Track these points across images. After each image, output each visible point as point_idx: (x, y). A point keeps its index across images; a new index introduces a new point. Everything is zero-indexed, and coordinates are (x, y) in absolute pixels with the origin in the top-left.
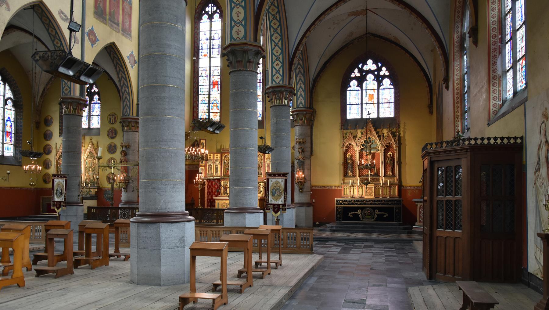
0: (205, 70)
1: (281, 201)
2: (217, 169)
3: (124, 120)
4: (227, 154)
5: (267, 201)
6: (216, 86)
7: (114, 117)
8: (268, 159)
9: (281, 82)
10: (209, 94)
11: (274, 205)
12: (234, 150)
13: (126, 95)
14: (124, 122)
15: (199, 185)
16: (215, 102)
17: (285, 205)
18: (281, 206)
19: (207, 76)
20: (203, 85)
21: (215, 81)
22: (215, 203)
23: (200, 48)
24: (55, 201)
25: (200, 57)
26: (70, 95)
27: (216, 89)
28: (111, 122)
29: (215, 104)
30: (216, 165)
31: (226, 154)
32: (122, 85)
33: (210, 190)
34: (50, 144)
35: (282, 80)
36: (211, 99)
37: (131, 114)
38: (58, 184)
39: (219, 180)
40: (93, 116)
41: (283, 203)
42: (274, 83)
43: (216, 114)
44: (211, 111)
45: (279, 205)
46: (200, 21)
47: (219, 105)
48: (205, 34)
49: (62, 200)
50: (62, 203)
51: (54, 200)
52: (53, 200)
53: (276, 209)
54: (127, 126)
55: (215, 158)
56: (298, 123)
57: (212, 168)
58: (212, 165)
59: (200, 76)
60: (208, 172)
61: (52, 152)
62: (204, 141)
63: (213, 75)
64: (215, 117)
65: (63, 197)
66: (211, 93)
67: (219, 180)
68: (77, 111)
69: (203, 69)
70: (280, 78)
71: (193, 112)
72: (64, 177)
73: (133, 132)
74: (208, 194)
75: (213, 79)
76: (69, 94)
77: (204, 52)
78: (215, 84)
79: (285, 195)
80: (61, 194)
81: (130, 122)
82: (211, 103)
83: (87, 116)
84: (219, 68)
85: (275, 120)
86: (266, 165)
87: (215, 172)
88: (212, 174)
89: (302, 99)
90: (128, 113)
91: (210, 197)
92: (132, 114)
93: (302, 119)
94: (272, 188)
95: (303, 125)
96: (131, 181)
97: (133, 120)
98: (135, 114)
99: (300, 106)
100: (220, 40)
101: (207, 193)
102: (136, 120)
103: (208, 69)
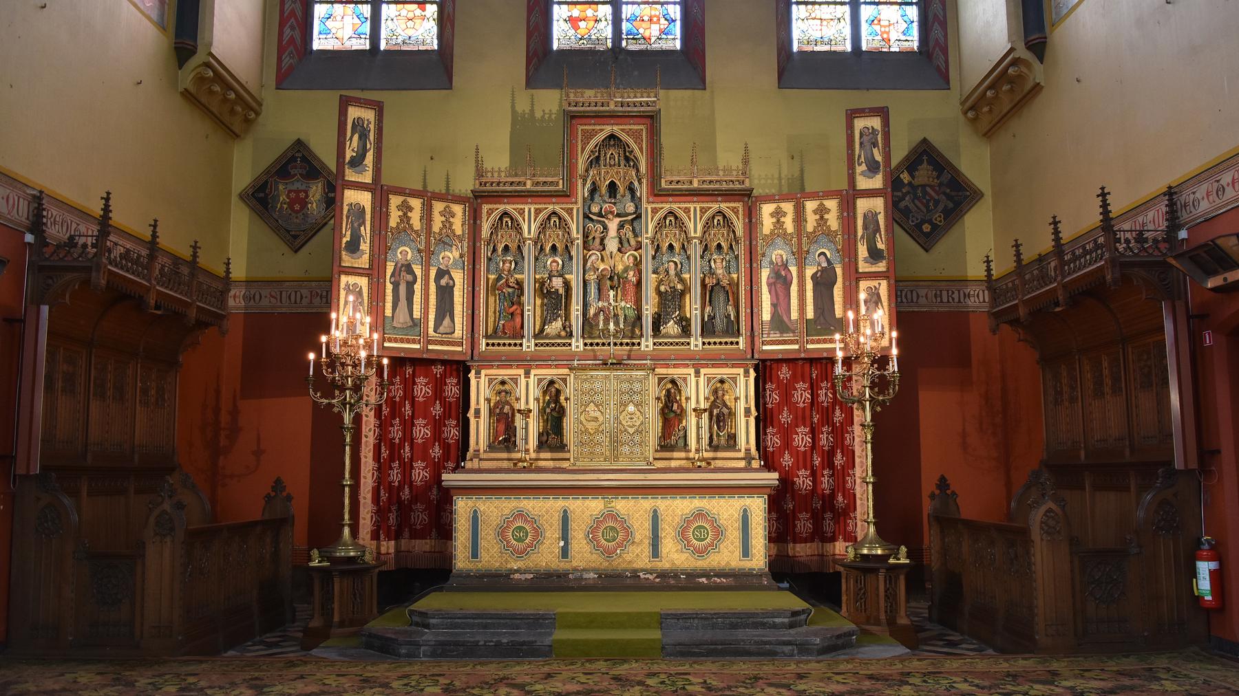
2: (445, 294)
4: (509, 208)
15: (343, 389)
30: (441, 274)
31: (502, 207)
33: (396, 433)
39: (460, 369)
55: (437, 225)
57: (417, 287)
58: (418, 270)
60: (388, 312)
64: (410, 24)
67: (460, 369)
74: (385, 453)
86: (765, 274)
87: (432, 316)
88: (415, 324)
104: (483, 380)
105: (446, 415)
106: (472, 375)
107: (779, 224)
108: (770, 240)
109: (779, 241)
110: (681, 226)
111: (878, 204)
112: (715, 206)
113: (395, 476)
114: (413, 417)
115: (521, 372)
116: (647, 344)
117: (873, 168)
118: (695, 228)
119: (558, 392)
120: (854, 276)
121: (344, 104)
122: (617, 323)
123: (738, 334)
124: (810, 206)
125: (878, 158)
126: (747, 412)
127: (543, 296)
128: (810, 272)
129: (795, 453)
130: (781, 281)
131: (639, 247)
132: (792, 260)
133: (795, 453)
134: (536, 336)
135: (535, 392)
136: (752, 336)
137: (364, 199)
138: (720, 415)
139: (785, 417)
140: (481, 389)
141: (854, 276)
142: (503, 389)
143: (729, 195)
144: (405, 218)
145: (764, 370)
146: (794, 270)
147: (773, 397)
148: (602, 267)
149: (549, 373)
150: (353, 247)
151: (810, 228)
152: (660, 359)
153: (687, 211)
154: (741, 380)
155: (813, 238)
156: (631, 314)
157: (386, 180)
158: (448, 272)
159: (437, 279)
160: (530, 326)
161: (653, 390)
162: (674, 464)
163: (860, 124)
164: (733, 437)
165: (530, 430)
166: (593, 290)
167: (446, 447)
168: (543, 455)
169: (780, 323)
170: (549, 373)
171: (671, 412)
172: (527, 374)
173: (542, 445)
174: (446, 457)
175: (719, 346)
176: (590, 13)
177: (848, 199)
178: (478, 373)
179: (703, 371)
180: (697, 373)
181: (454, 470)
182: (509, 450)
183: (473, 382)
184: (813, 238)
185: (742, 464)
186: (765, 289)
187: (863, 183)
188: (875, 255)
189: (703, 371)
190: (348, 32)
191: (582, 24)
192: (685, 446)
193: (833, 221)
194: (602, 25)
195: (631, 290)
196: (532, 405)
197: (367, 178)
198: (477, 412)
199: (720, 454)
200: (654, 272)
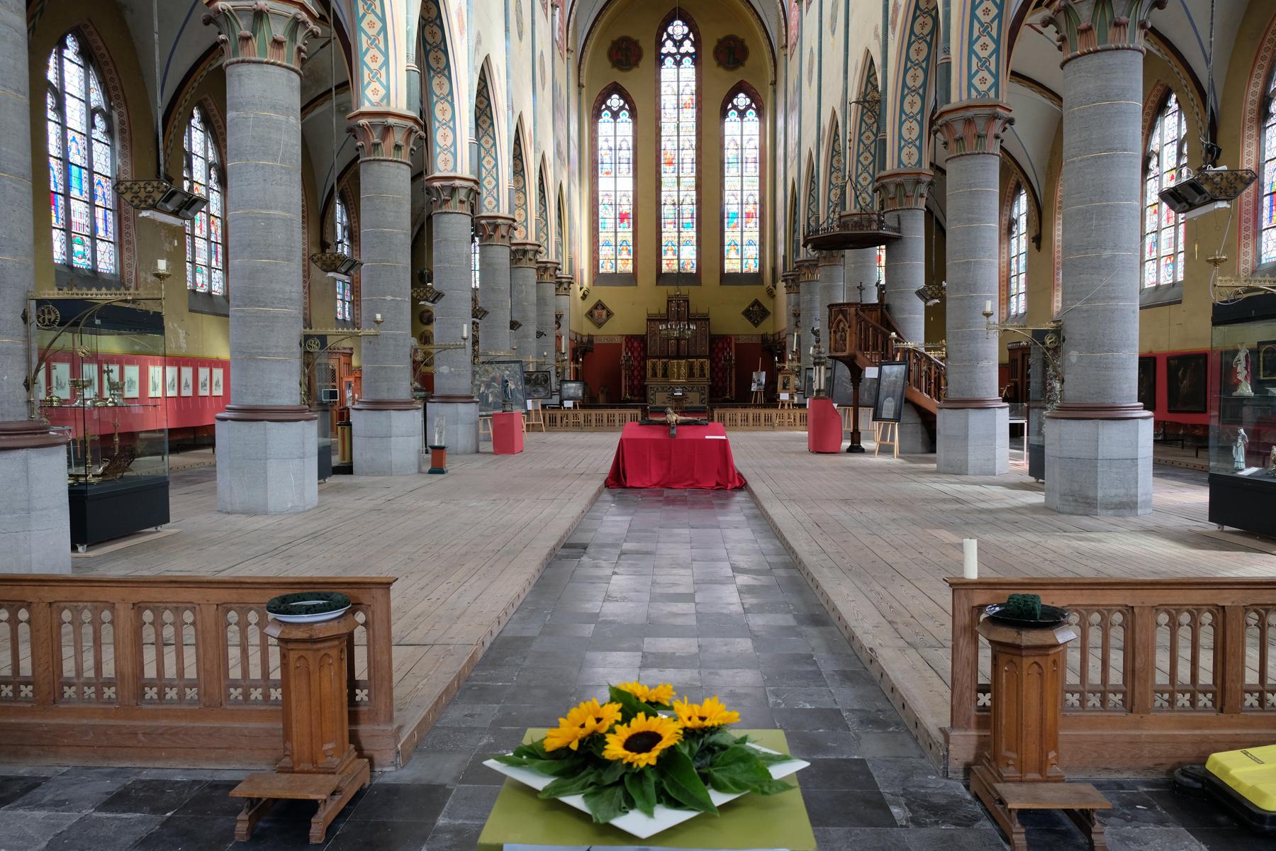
6: (626, 221)
10: (616, 232)
19: (611, 204)
23: (600, 162)
25: (600, 175)
36: (619, 239)
44: (618, 257)
46: (599, 119)
47: (631, 248)
48: (607, 141)
66: (618, 230)
69: (605, 193)
77: (603, 169)
78: (623, 217)
100: (631, 151)
103: (613, 193)
138: (702, 369)
142: (654, 365)
165: (660, 373)
190: (609, 267)
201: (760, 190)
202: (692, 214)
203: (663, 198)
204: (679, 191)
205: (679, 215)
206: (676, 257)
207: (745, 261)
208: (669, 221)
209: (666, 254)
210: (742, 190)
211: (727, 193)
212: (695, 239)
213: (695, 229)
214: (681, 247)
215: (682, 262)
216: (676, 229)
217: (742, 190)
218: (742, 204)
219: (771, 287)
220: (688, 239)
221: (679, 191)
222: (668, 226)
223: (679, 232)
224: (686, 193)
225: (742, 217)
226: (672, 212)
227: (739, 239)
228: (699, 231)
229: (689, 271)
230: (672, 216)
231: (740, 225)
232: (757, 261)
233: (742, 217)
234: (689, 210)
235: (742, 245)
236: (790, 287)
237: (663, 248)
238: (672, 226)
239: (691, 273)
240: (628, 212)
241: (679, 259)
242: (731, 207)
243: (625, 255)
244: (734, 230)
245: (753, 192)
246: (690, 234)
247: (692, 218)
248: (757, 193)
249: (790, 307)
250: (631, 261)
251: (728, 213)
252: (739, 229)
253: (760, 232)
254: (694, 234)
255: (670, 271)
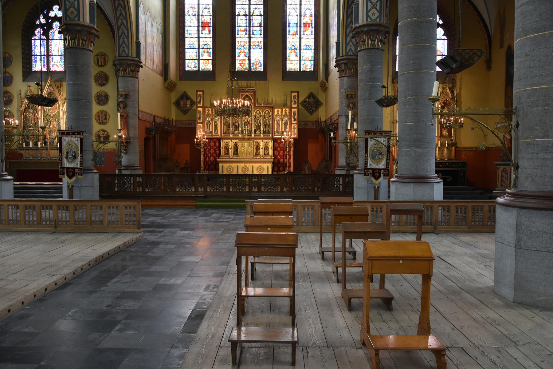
0: (192, 7)
1: (383, 165)
2: (216, 126)
3: (121, 62)
5: (366, 166)
6: (207, 28)
7: (103, 57)
8: (277, 115)
9: (378, 20)
10: (199, 37)
11: (374, 170)
12: (414, 99)
13: (123, 29)
14: (120, 64)
16: (206, 47)
17: (388, 170)
18: (382, 171)
19: (195, 15)
20: (190, 26)
21: (205, 22)
22: (218, 166)
24: (64, 168)
26: (79, 20)
27: (206, 31)
28: (100, 64)
29: (206, 50)
30: (215, 122)
32: (118, 16)
34: (10, 91)
35: (380, 17)
36: (201, 43)
37: (130, 55)
38: (69, 144)
39: (219, 140)
40: (52, 55)
41: (385, 167)
42: (369, 20)
43: (208, 62)
44: (201, 58)
45: (380, 170)
47: (211, 51)
49: (76, 166)
50: (76, 170)
51: (63, 166)
52: (62, 166)
53: (377, 175)
54: (125, 70)
56: (346, 73)
57: (211, 125)
58: (211, 122)
59: (186, 14)
60: (206, 130)
61: (13, 102)
62: (201, 93)
63: (203, 14)
64: (206, 64)
65: (78, 161)
66: (201, 35)
67: (219, 140)
68: (87, 44)
69: (190, 6)
70: (377, 14)
71: (180, 59)
72: (79, 134)
73: (132, 78)
74: (205, 155)
75: (203, 20)
76: (77, 19)
79: (387, 157)
80: (75, 157)
81: (129, 65)
82: (200, 48)
83: (62, 55)
84: (211, 6)
85: (369, 66)
86: (275, 122)
87: (214, 130)
88: (211, 132)
89: (352, 45)
90: (125, 53)
91: (207, 159)
92: (132, 55)
93: (351, 70)
94: (372, 149)
95: (352, 76)
96: (132, 140)
97: (133, 63)
98: (134, 55)
99: (349, 54)
101: (204, 154)
102: (136, 63)
103: (196, 6)
104: (223, 142)
105: (216, 148)
106: (221, 141)
107: (278, 113)
108: (276, 116)
109: (278, 116)
110: (260, 113)
111: (296, 110)
112: (266, 109)
113: (207, 159)
114: (210, 149)
115: (230, 141)
116: (253, 135)
117: (295, 103)
118: (262, 113)
119: (237, 144)
120: (291, 124)
121: (197, 91)
122: (247, 132)
123: (270, 134)
124: (284, 109)
125: (296, 101)
126: (271, 148)
127: (234, 126)
128: (283, 122)
129: (280, 156)
130: (278, 124)
131: (252, 117)
132: (280, 120)
133: (280, 156)
134: (233, 134)
135: (233, 144)
136: (273, 134)
137: (201, 109)
138: (266, 149)
139: (279, 149)
140: (223, 144)
141: (291, 124)
142: (227, 144)
143: (269, 107)
144: (208, 112)
145: (275, 141)
146: (280, 122)
147: (277, 145)
148: (245, 120)
149: (235, 141)
150: (199, 118)
151: (284, 114)
152: (255, 138)
153: (261, 110)
154: (270, 142)
155: (284, 116)
156: (251, 130)
157: (205, 105)
158: (216, 122)
159: (214, 124)
160: (231, 132)
161: (253, 144)
162: (258, 158)
163: (293, 94)
164: (268, 153)
165: (232, 151)
166: (243, 125)
167: (216, 154)
168: (234, 156)
169: (278, 132)
170: (235, 141)
171: (258, 148)
172: (231, 141)
173: (234, 154)
174: (217, 156)
175: (267, 136)
176: (244, 62)
177: (291, 108)
178: (222, 141)
179: (263, 141)
180: (262, 141)
181: (218, 159)
182: (228, 155)
183: (221, 142)
184: (284, 116)
185: (270, 158)
186: (275, 125)
187: (293, 106)
188: (295, 120)
189: (263, 141)
190: (193, 66)
191: (242, 65)
192: (260, 155)
193: (288, 113)
194: (246, 65)
195: (250, 125)
196: (232, 147)
197: (201, 105)
198: (222, 148)
199: (266, 156)
200: (255, 121)
201: (315, 5)
202: (261, 24)
203: (237, 11)
204: (250, 4)
205: (250, 25)
206: (247, 58)
207: (302, 62)
208: (242, 29)
209: (239, 56)
210: (301, 5)
211: (288, 7)
212: (262, 44)
213: (262, 36)
214: (252, 50)
215: (252, 62)
216: (247, 36)
217: (301, 5)
218: (300, 16)
219: (324, 81)
220: (257, 44)
221: (250, 4)
222: (240, 33)
223: (250, 38)
224: (255, 6)
225: (300, 27)
226: (244, 22)
227: (298, 44)
228: (265, 38)
229: (258, 70)
230: (244, 25)
231: (299, 33)
232: (312, 62)
233: (300, 27)
234: (258, 20)
235: (300, 49)
236: (343, 71)
237: (237, 51)
238: (244, 33)
239: (260, 72)
240: (209, 21)
241: (249, 60)
242: (292, 19)
243: (206, 56)
244: (294, 37)
245: (309, 7)
246: (258, 38)
247: (260, 26)
248: (313, 7)
249: (343, 90)
250: (211, 61)
251: (289, 23)
252: (298, 36)
253: (315, 38)
254: (262, 40)
255: (243, 69)
